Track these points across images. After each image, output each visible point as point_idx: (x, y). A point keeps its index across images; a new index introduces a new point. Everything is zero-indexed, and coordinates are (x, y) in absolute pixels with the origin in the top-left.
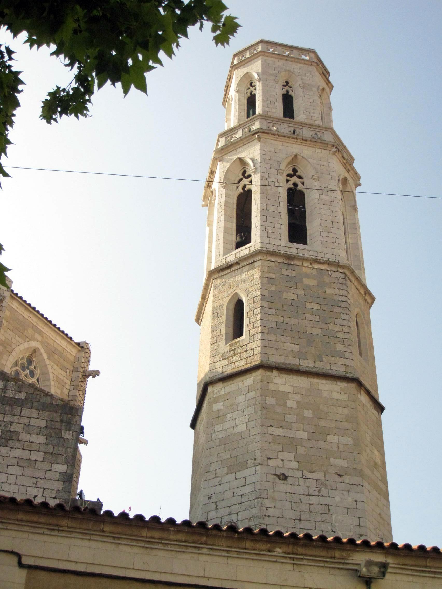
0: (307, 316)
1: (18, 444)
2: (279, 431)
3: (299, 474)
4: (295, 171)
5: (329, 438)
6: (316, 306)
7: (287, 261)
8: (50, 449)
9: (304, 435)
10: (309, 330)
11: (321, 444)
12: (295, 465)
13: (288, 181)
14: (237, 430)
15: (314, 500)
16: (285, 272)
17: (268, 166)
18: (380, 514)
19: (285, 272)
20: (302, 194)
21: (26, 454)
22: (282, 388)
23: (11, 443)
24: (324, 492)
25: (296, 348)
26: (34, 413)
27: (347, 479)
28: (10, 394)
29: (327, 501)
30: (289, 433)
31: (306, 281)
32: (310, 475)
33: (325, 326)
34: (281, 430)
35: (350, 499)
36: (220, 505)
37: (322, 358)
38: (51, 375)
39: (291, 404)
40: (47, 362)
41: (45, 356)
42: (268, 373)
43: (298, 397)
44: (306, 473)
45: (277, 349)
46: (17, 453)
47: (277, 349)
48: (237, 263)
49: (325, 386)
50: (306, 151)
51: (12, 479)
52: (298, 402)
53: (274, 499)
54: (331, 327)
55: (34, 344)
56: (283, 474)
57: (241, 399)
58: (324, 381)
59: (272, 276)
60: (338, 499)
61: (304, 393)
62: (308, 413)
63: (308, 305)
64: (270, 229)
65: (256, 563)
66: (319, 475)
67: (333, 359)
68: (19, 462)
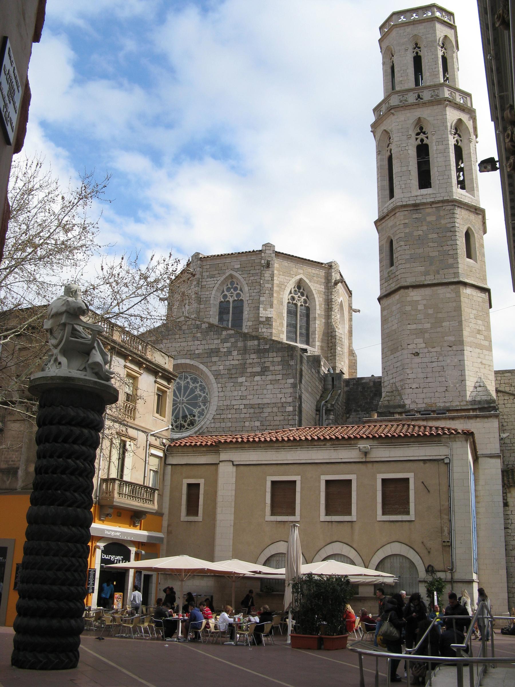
0: (429, 244)
1: (269, 373)
2: (414, 326)
3: (426, 350)
4: (421, 128)
5: (444, 324)
6: (435, 236)
7: (415, 208)
8: (285, 372)
9: (428, 326)
10: (431, 254)
11: (439, 330)
12: (423, 345)
13: (417, 139)
14: (394, 328)
15: (435, 364)
16: (415, 216)
17: (400, 134)
18: (481, 363)
19: (415, 216)
20: (426, 147)
21: (274, 377)
22: (415, 298)
23: (266, 373)
24: (441, 358)
25: (422, 269)
26: (275, 354)
27: (454, 348)
28: (262, 347)
29: (443, 364)
30: (420, 326)
31: (429, 219)
32: (432, 350)
33: (440, 249)
34: (415, 325)
35: (456, 360)
36: (389, 373)
37: (439, 271)
38: (314, 292)
39: (421, 307)
40: (310, 284)
41: (307, 281)
42: (406, 291)
43: (425, 302)
44: (430, 349)
45: (411, 273)
46: (270, 377)
47: (411, 273)
48: (387, 215)
49: (441, 290)
50: (425, 113)
51: (269, 392)
52: (424, 305)
53: (412, 368)
54: (445, 248)
55: (298, 277)
56: (417, 352)
57: (394, 308)
58: (440, 288)
59: (407, 221)
60: (449, 361)
61: (428, 298)
62: (430, 311)
63: (430, 236)
64: (403, 186)
65: (319, 451)
66: (438, 349)
67: (446, 270)
68: (272, 382)
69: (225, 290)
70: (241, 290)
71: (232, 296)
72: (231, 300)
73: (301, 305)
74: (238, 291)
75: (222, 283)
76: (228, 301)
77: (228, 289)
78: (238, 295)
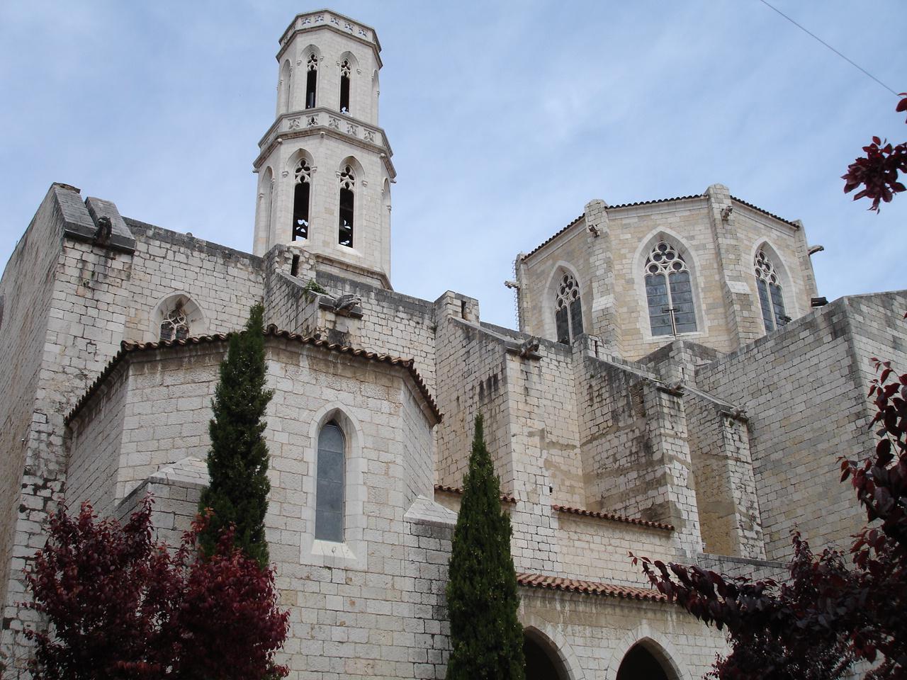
69: (652, 258)
70: (680, 257)
71: (665, 268)
72: (666, 272)
73: (770, 284)
74: (676, 259)
75: (647, 247)
76: (661, 275)
77: (657, 257)
78: (677, 265)
